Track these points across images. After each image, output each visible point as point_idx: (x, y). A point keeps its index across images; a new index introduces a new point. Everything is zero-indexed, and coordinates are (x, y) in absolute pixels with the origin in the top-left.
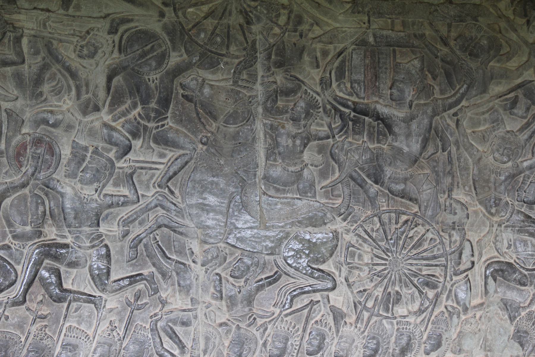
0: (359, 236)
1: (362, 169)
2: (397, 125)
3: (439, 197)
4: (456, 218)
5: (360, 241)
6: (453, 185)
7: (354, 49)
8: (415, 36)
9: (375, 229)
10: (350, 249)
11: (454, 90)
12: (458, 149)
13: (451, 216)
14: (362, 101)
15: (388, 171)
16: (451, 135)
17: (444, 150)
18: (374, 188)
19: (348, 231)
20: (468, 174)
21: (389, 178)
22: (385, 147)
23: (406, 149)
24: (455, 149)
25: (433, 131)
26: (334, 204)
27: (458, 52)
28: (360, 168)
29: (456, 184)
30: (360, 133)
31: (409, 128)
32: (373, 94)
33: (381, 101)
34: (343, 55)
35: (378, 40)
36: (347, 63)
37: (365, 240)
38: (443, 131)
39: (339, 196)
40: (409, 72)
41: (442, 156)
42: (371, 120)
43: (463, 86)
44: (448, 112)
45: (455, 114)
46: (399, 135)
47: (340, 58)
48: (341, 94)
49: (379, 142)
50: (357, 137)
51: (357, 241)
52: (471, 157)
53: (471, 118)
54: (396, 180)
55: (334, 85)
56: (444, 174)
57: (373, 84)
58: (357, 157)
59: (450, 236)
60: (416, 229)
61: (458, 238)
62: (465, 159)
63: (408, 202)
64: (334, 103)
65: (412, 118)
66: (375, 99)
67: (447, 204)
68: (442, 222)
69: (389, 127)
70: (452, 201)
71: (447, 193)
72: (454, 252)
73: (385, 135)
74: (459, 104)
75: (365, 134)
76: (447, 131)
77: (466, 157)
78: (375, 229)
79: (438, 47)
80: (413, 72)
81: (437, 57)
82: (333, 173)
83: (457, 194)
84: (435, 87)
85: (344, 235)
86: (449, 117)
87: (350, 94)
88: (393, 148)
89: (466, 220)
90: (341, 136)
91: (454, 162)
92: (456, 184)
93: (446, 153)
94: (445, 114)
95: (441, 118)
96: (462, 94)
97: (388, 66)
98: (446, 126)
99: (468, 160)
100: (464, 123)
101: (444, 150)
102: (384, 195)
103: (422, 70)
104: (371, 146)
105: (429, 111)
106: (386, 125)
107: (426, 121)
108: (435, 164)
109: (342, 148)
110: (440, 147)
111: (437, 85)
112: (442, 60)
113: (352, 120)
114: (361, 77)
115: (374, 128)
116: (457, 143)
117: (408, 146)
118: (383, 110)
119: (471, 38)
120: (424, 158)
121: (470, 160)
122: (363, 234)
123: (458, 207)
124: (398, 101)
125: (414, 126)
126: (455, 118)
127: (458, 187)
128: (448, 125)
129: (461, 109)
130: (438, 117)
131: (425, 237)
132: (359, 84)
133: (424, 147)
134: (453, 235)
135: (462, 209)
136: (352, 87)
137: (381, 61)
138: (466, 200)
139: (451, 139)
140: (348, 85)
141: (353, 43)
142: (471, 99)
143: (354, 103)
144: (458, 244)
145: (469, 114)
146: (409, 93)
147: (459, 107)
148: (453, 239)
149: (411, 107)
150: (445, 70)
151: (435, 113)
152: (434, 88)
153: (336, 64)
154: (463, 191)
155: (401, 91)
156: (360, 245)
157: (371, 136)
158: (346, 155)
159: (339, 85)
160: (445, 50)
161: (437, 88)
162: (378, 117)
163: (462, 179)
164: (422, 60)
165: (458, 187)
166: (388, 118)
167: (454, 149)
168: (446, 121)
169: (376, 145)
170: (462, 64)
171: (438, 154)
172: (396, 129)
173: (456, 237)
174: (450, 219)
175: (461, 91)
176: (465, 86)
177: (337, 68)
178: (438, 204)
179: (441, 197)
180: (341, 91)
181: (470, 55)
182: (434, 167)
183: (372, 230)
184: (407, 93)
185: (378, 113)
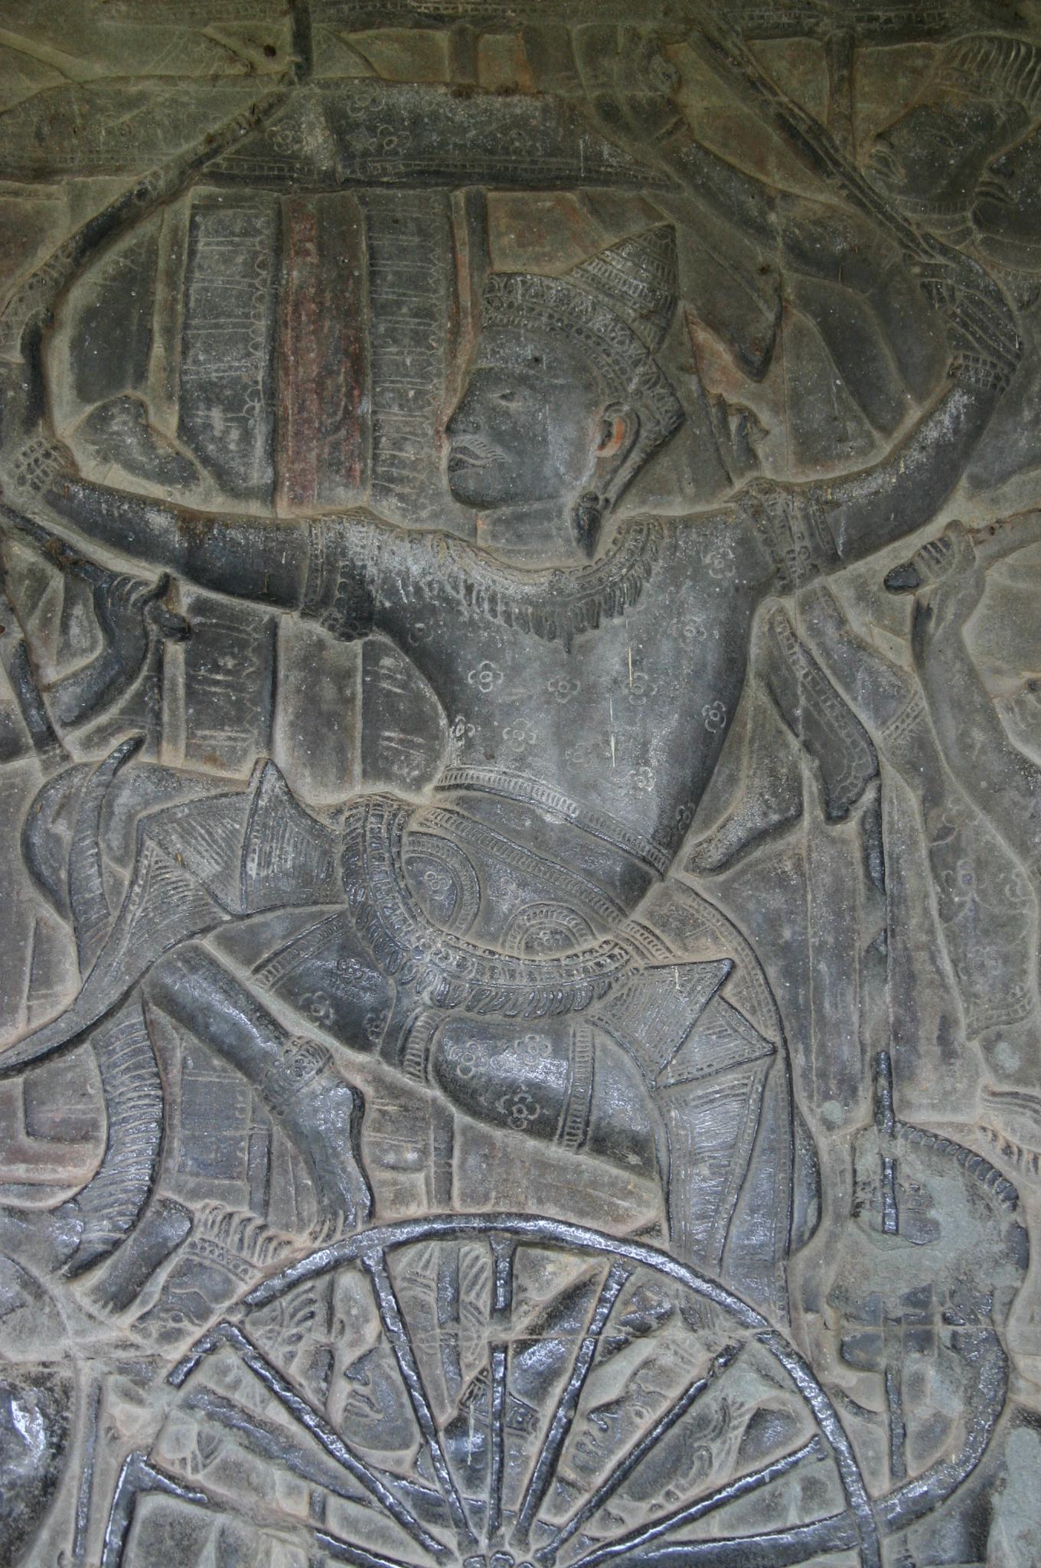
0: (222, 1410)
1: (244, 946)
2: (489, 651)
3: (813, 1124)
4: (936, 1262)
5: (231, 1449)
6: (911, 1041)
7: (208, 206)
8: (609, 112)
9: (347, 1357)
10: (148, 1505)
11: (887, 430)
12: (933, 798)
13: (901, 1253)
14: (255, 509)
15: (434, 960)
16: (878, 702)
17: (835, 811)
18: (330, 1080)
19: (137, 1380)
20: (1006, 959)
21: (441, 1002)
22: (425, 798)
23: (556, 804)
24: (913, 799)
25: (755, 693)
26: (34, 1188)
27: (904, 207)
28: (227, 942)
29: (929, 1029)
30: (249, 712)
31: (575, 671)
32: (332, 465)
33: (389, 508)
34: (128, 241)
35: (361, 142)
36: (161, 292)
37: (264, 1443)
38: (818, 686)
39: (83, 1133)
40: (566, 326)
41: (822, 848)
42: (317, 629)
43: (943, 401)
44: (859, 567)
45: (901, 580)
46: (510, 710)
47: (112, 259)
48: (117, 477)
49: (377, 766)
50: (220, 738)
51: (208, 1448)
52: (1024, 849)
53: (1009, 600)
54: (485, 1016)
55: (67, 416)
56: (843, 972)
57: (331, 399)
58: (208, 867)
59: (894, 1390)
60: (645, 1348)
61: (955, 1407)
62: (980, 864)
63: (587, 1161)
64: (59, 528)
65: (598, 606)
66: (348, 497)
67: (868, 1163)
68: (839, 1295)
69: (437, 666)
70: (900, 1147)
71: (865, 1092)
72: (921, 1510)
73: (419, 724)
74: (928, 514)
75: (282, 721)
76: (848, 687)
77: (991, 848)
78: (347, 1357)
79: (776, 180)
80: (600, 322)
81: (763, 231)
82: (44, 979)
83: (945, 1100)
84: (765, 417)
85: (117, 1408)
86: (861, 595)
87: (180, 473)
88: (468, 799)
89: (1007, 1277)
90: (104, 733)
91: (911, 885)
92: (929, 1029)
93: (850, 828)
94: (838, 583)
95: (806, 606)
96: (941, 447)
97: (439, 300)
98: (841, 651)
99: (1008, 867)
100: (968, 632)
101: (835, 811)
102: (411, 1115)
103: (662, 310)
104: (318, 796)
105: (719, 559)
106: (414, 646)
107: (697, 624)
108: (776, 901)
109: (104, 810)
110: (811, 787)
111: (776, 408)
112: (798, 252)
113: (183, 632)
114: (250, 367)
115: (343, 677)
116: (920, 760)
117: (580, 787)
118: (397, 553)
119: (986, 122)
120: (695, 866)
121: (1022, 868)
122: (249, 1394)
123: (947, 1190)
124: (495, 501)
125: (612, 652)
126: (908, 600)
127: (949, 1053)
128: (859, 646)
129: (938, 548)
130: (790, 603)
131: (710, 1402)
132: (232, 406)
133: (692, 794)
134: (918, 1380)
135: (974, 1195)
136: (185, 429)
137: (389, 268)
138: (1005, 1134)
139: (877, 736)
140: (166, 421)
141: (191, 168)
142: (1004, 478)
143: (186, 519)
144: (952, 1448)
145: (997, 576)
146: (576, 453)
147: (931, 531)
148: (919, 1414)
149: (589, 531)
150: (823, 316)
151: (762, 579)
152: (748, 418)
153: (81, 295)
154: (987, 1078)
155: (519, 439)
156: (230, 1472)
157: (320, 731)
158: (132, 851)
159: (98, 422)
160: (819, 197)
161: (775, 426)
162: (361, 610)
163: (970, 996)
164: (663, 252)
165: (949, 1053)
166: (425, 611)
167: (904, 800)
168: (842, 622)
169: (360, 789)
170: (934, 270)
171: (800, 836)
172: (486, 680)
173: (940, 1395)
174: (888, 1268)
175: (932, 434)
176: (959, 401)
177: (89, 315)
178: (802, 1172)
179: (830, 1126)
180: (109, 453)
181: (986, 219)
182: (773, 922)
183: (326, 1362)
184: (558, 456)
185: (357, 580)
